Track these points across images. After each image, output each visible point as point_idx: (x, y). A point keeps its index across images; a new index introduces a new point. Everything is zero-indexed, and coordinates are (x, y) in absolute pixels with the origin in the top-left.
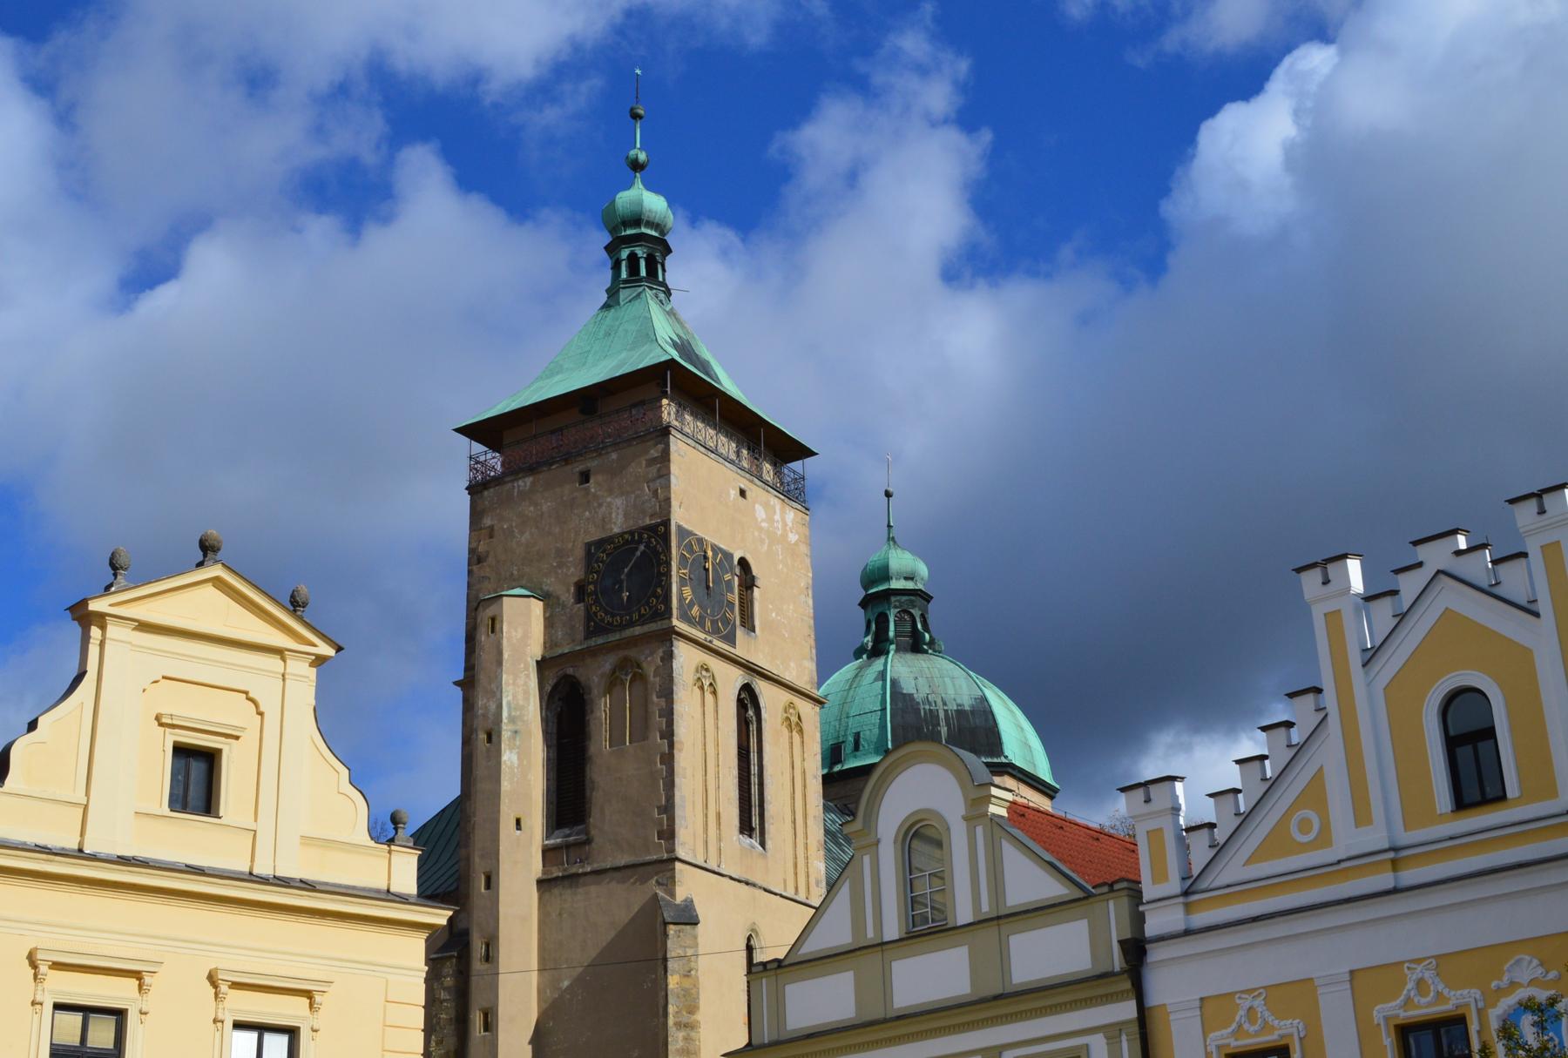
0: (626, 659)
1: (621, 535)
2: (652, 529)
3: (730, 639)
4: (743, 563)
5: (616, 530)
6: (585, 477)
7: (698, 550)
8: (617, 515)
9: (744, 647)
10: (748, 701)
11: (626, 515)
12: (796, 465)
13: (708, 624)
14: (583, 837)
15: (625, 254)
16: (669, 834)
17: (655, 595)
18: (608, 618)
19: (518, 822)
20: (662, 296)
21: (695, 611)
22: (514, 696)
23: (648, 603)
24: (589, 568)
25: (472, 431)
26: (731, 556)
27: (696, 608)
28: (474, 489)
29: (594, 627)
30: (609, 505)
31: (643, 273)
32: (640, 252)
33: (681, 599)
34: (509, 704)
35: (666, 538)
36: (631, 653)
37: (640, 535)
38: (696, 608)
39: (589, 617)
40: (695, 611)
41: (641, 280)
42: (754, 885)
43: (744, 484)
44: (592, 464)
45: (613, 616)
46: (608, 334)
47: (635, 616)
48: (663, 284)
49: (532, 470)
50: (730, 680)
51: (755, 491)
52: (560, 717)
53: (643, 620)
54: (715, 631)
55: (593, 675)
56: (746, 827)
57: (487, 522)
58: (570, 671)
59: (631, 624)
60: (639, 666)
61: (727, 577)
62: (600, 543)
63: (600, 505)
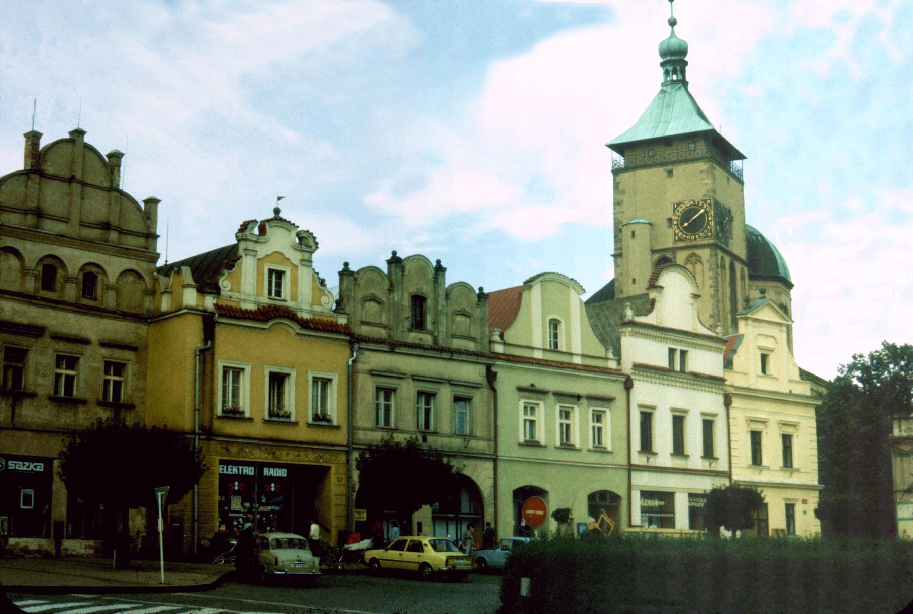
0: (693, 254)
6: (670, 173)
12: (737, 164)
28: (616, 172)
46: (668, 106)
57: (621, 187)
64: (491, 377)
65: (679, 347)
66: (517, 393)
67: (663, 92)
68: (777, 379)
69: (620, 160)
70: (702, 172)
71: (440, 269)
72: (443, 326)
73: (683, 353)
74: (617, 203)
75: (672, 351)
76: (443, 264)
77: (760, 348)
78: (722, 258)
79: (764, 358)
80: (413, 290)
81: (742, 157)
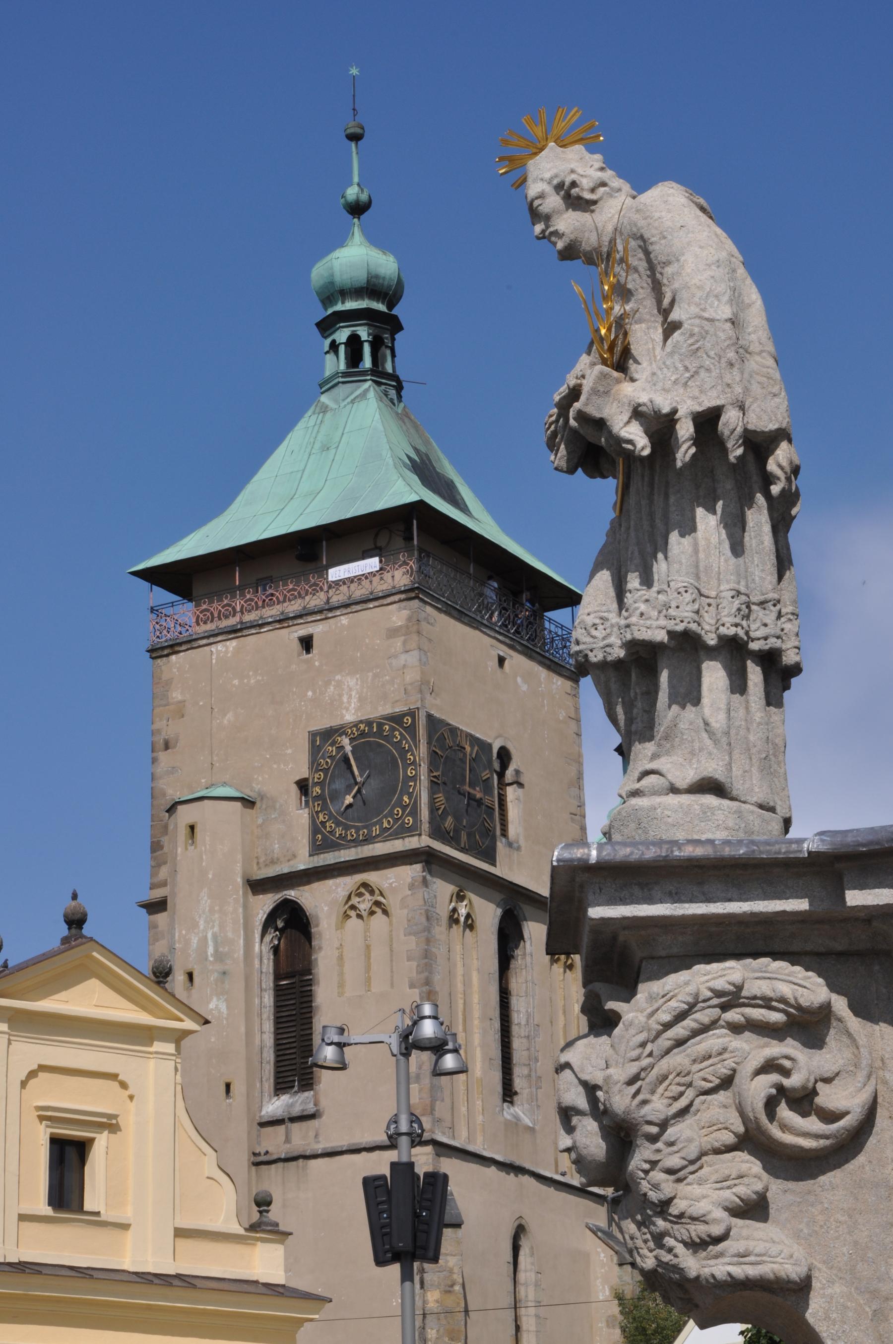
0: (365, 885)
1: (356, 725)
2: (396, 719)
3: (490, 856)
4: (504, 755)
5: (349, 717)
6: (307, 643)
11: (361, 699)
12: (560, 615)
13: (464, 837)
14: (311, 1108)
15: (342, 335)
17: (400, 803)
18: (338, 831)
19: (228, 1086)
20: (393, 393)
21: (449, 822)
22: (222, 927)
23: (391, 814)
24: (314, 764)
26: (490, 746)
27: (450, 820)
29: (320, 844)
30: (339, 684)
31: (367, 363)
32: (364, 333)
33: (433, 809)
34: (215, 937)
35: (412, 730)
36: (372, 877)
37: (380, 726)
38: (450, 820)
39: (315, 829)
40: (449, 822)
41: (364, 373)
42: (518, 1170)
43: (503, 650)
44: (317, 629)
45: (347, 828)
46: (326, 448)
47: (376, 830)
48: (394, 377)
49: (234, 632)
51: (517, 661)
52: (276, 950)
53: (388, 835)
55: (321, 900)
56: (508, 1093)
58: (291, 894)
59: (368, 840)
60: (382, 894)
61: (485, 775)
62: (329, 734)
63: (328, 683)
68: (125, 1227)
70: (393, 633)
77: (46, 1116)
79: (68, 1158)
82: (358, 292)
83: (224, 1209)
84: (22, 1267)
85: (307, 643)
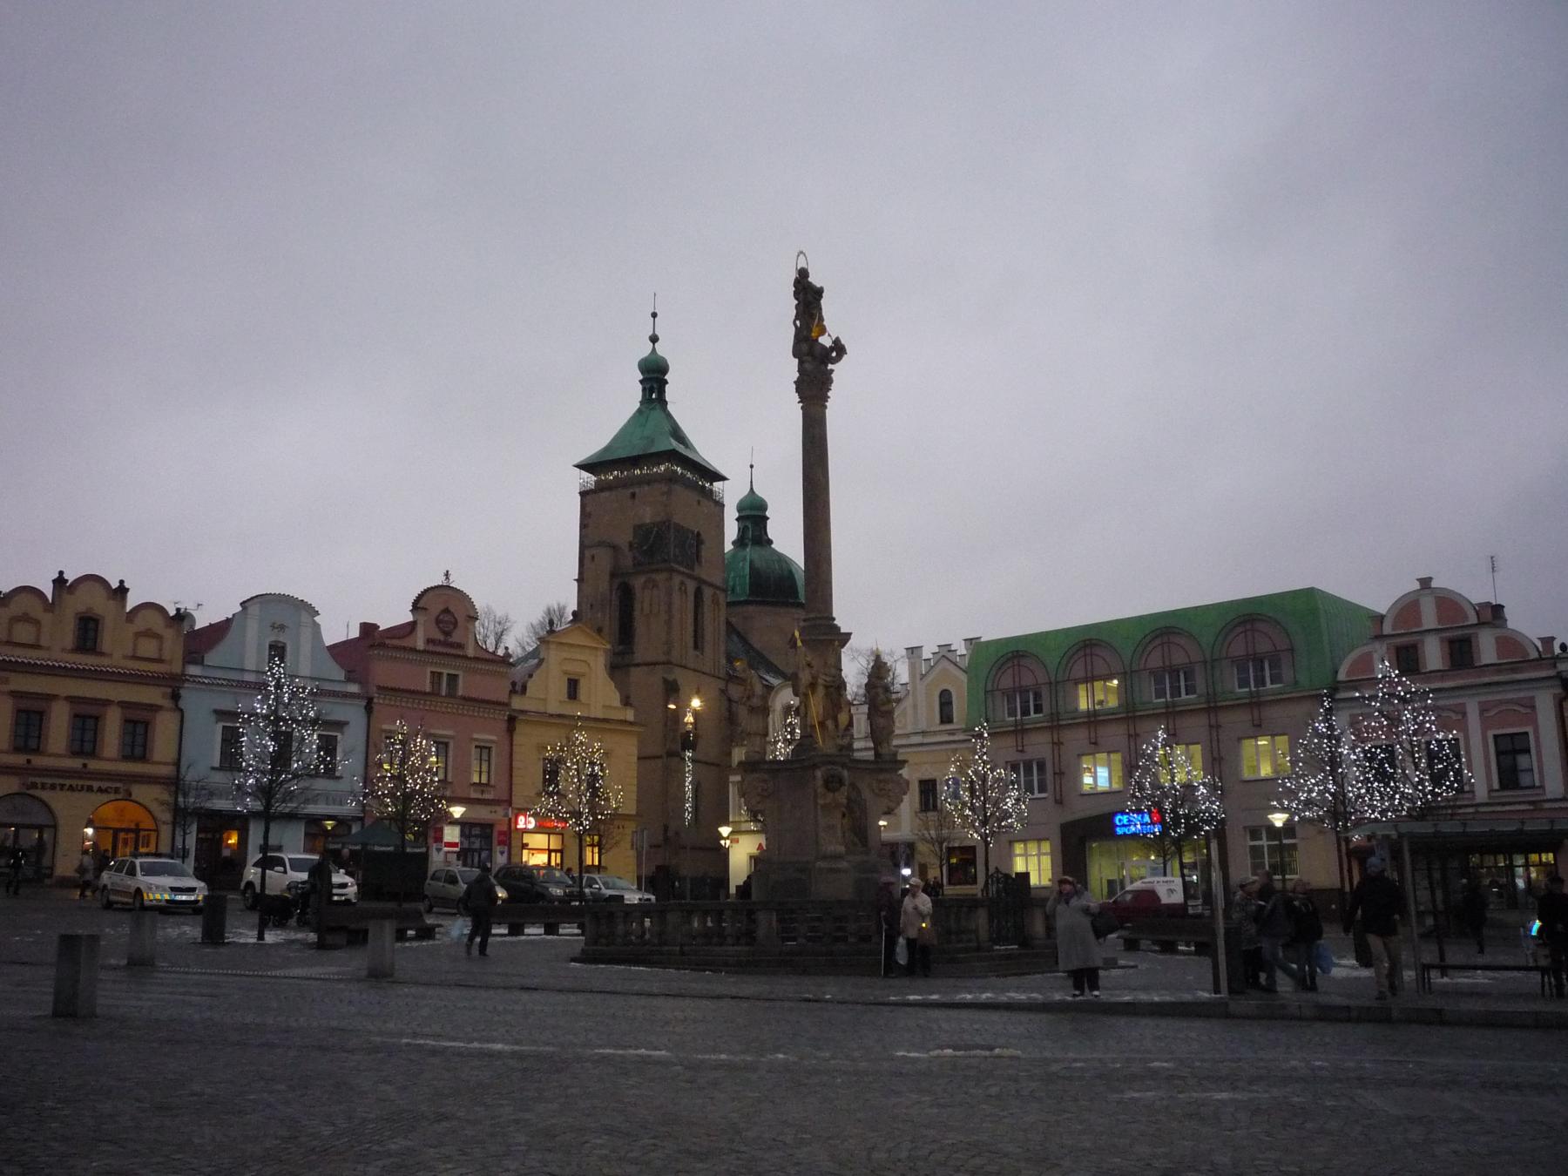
6: (633, 495)
7: (680, 529)
8: (647, 515)
9: (698, 571)
10: (698, 594)
12: (717, 485)
16: (668, 653)
25: (582, 466)
28: (583, 494)
36: (654, 576)
50: (691, 586)
54: (687, 567)
55: (638, 582)
56: (696, 647)
64: (176, 697)
65: (445, 671)
66: (213, 718)
67: (639, 411)
69: (589, 479)
71: (122, 591)
72: (116, 646)
73: (453, 679)
74: (583, 526)
75: (436, 676)
76: (126, 585)
77: (565, 673)
78: (682, 583)
79: (573, 687)
80: (81, 608)
81: (723, 479)
82: (654, 371)
83: (615, 699)
84: (560, 716)
85: (633, 495)
